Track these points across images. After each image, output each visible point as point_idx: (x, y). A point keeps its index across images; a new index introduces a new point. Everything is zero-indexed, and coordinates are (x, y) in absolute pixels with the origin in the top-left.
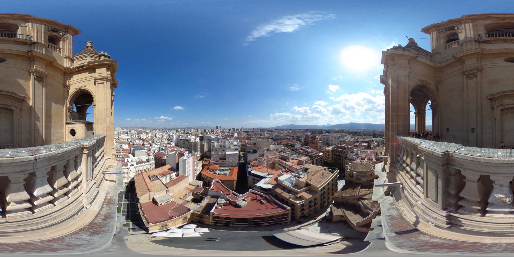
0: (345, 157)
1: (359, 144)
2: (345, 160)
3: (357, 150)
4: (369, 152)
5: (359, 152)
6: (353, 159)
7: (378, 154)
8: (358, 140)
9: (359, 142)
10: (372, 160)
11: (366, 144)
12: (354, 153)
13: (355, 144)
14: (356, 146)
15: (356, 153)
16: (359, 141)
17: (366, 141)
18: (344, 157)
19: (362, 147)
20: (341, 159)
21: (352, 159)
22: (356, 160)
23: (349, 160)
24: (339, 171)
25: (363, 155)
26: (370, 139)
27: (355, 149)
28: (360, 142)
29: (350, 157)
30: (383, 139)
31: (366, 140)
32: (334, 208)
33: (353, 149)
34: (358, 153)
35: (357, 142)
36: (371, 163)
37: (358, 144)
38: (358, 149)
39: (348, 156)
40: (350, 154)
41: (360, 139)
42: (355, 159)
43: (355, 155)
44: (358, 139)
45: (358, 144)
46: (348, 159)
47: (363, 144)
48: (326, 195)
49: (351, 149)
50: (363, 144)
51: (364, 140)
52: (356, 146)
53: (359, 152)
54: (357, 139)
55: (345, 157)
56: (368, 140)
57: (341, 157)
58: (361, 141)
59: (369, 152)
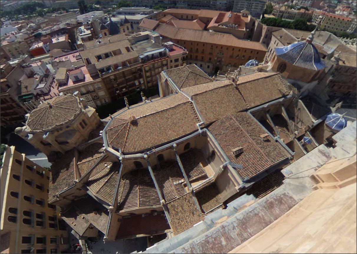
0: (20, 97)
1: (44, 43)
2: (24, 105)
3: (39, 64)
4: (73, 60)
5: (49, 66)
6: (42, 91)
7: (93, 63)
8: (40, 31)
9: (43, 38)
10: (84, 80)
11: (62, 39)
12: (38, 77)
13: (35, 46)
14: (40, 51)
15: (41, 73)
16: (44, 33)
17: (63, 29)
18: (16, 98)
19: (56, 50)
20: (14, 104)
21: (40, 93)
22: (50, 91)
23: (33, 100)
24: (13, 148)
25: (61, 75)
26: (73, 21)
27: (34, 65)
28: (45, 36)
29: (31, 90)
30: (105, 13)
31: (62, 26)
32: (71, 221)
33: (27, 66)
34: (47, 70)
35: (38, 37)
36: (76, 95)
37: (41, 44)
38: (40, 60)
39: (24, 92)
40: (27, 84)
41: (44, 25)
42: (46, 91)
43: (41, 81)
44: (39, 27)
45: (41, 44)
46: (31, 98)
47: (54, 41)
48: (37, 209)
49: (23, 67)
50: (54, 41)
51: (55, 28)
52: (40, 51)
53: (49, 66)
54: (36, 30)
55: (20, 97)
56: (68, 24)
57: (9, 100)
58: (48, 31)
59: (73, 60)
